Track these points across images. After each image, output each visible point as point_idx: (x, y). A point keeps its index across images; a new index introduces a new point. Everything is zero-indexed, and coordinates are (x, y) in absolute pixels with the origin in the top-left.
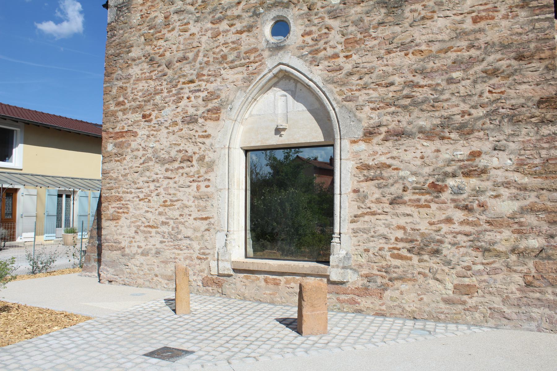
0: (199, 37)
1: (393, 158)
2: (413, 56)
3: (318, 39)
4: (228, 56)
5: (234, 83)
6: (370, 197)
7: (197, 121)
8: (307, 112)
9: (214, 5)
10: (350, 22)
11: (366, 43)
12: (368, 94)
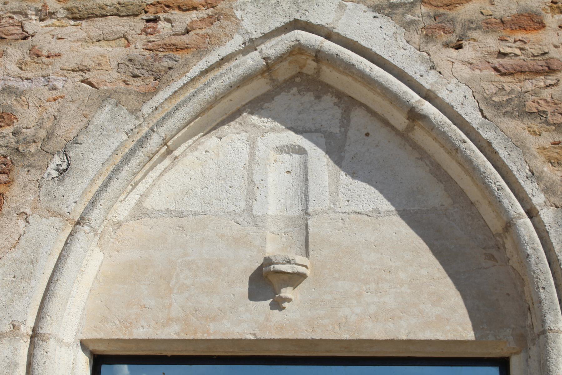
5: (87, 76)
8: (397, 219)
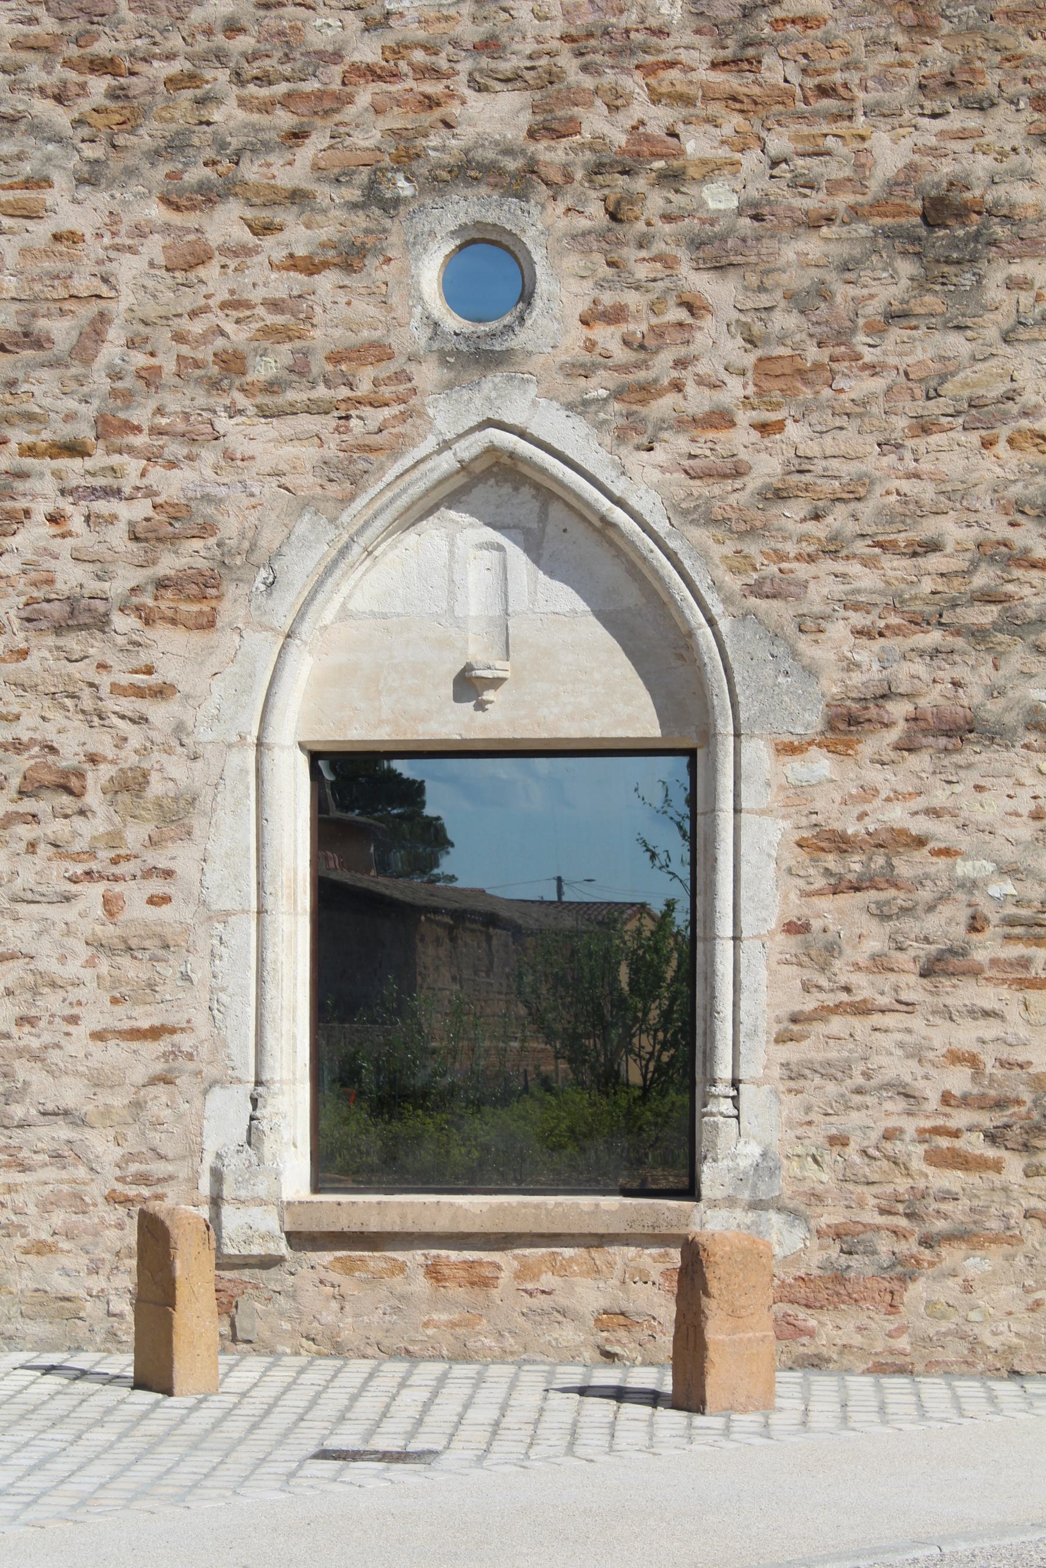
0: (102, 254)
1: (934, 813)
2: (1011, 453)
3: (651, 342)
4: (249, 362)
5: (283, 480)
6: (848, 950)
7: (108, 623)
8: (593, 619)
9: (172, 119)
10: (778, 295)
11: (840, 383)
12: (844, 575)
